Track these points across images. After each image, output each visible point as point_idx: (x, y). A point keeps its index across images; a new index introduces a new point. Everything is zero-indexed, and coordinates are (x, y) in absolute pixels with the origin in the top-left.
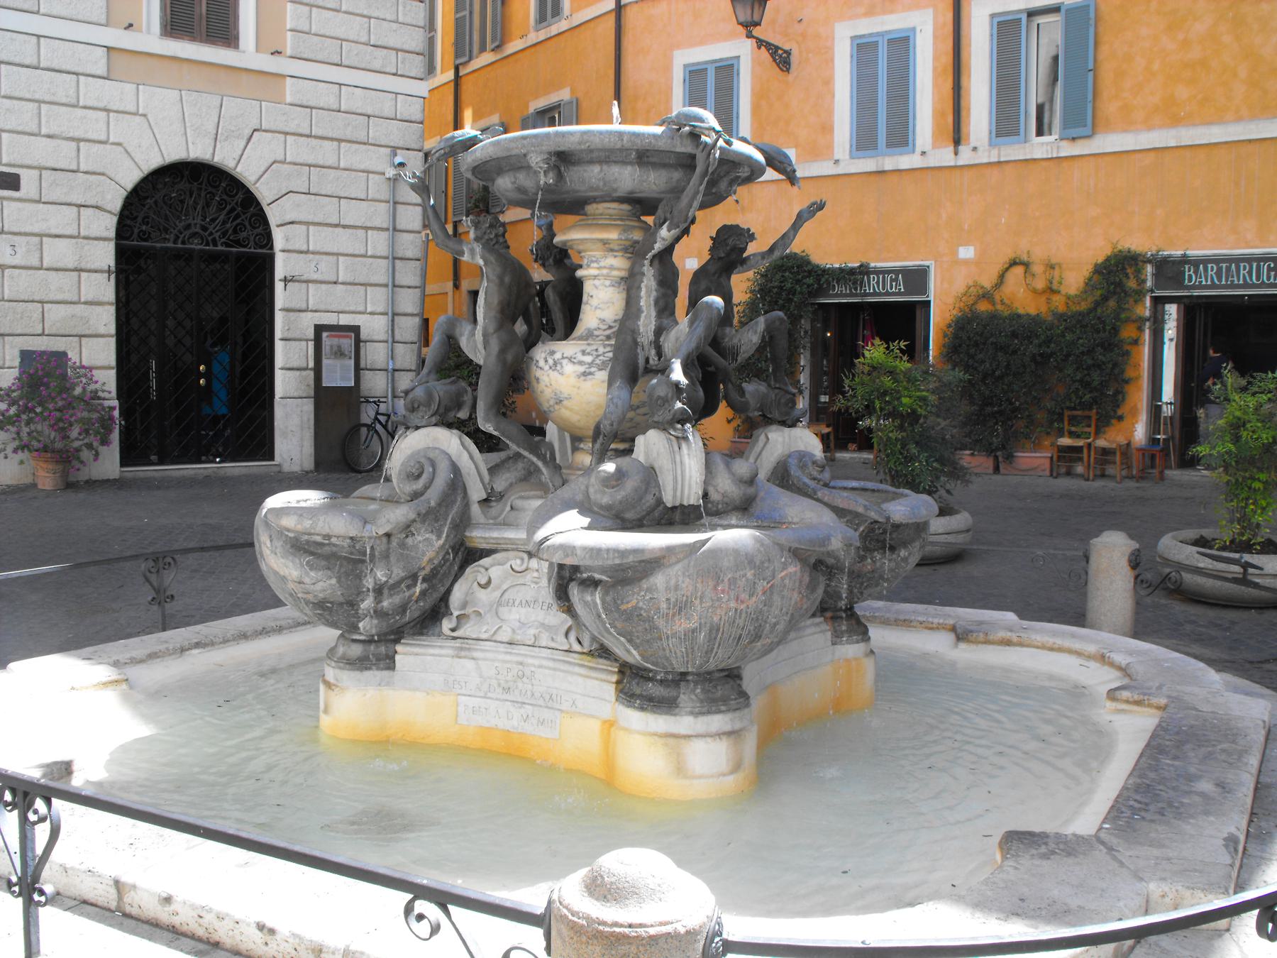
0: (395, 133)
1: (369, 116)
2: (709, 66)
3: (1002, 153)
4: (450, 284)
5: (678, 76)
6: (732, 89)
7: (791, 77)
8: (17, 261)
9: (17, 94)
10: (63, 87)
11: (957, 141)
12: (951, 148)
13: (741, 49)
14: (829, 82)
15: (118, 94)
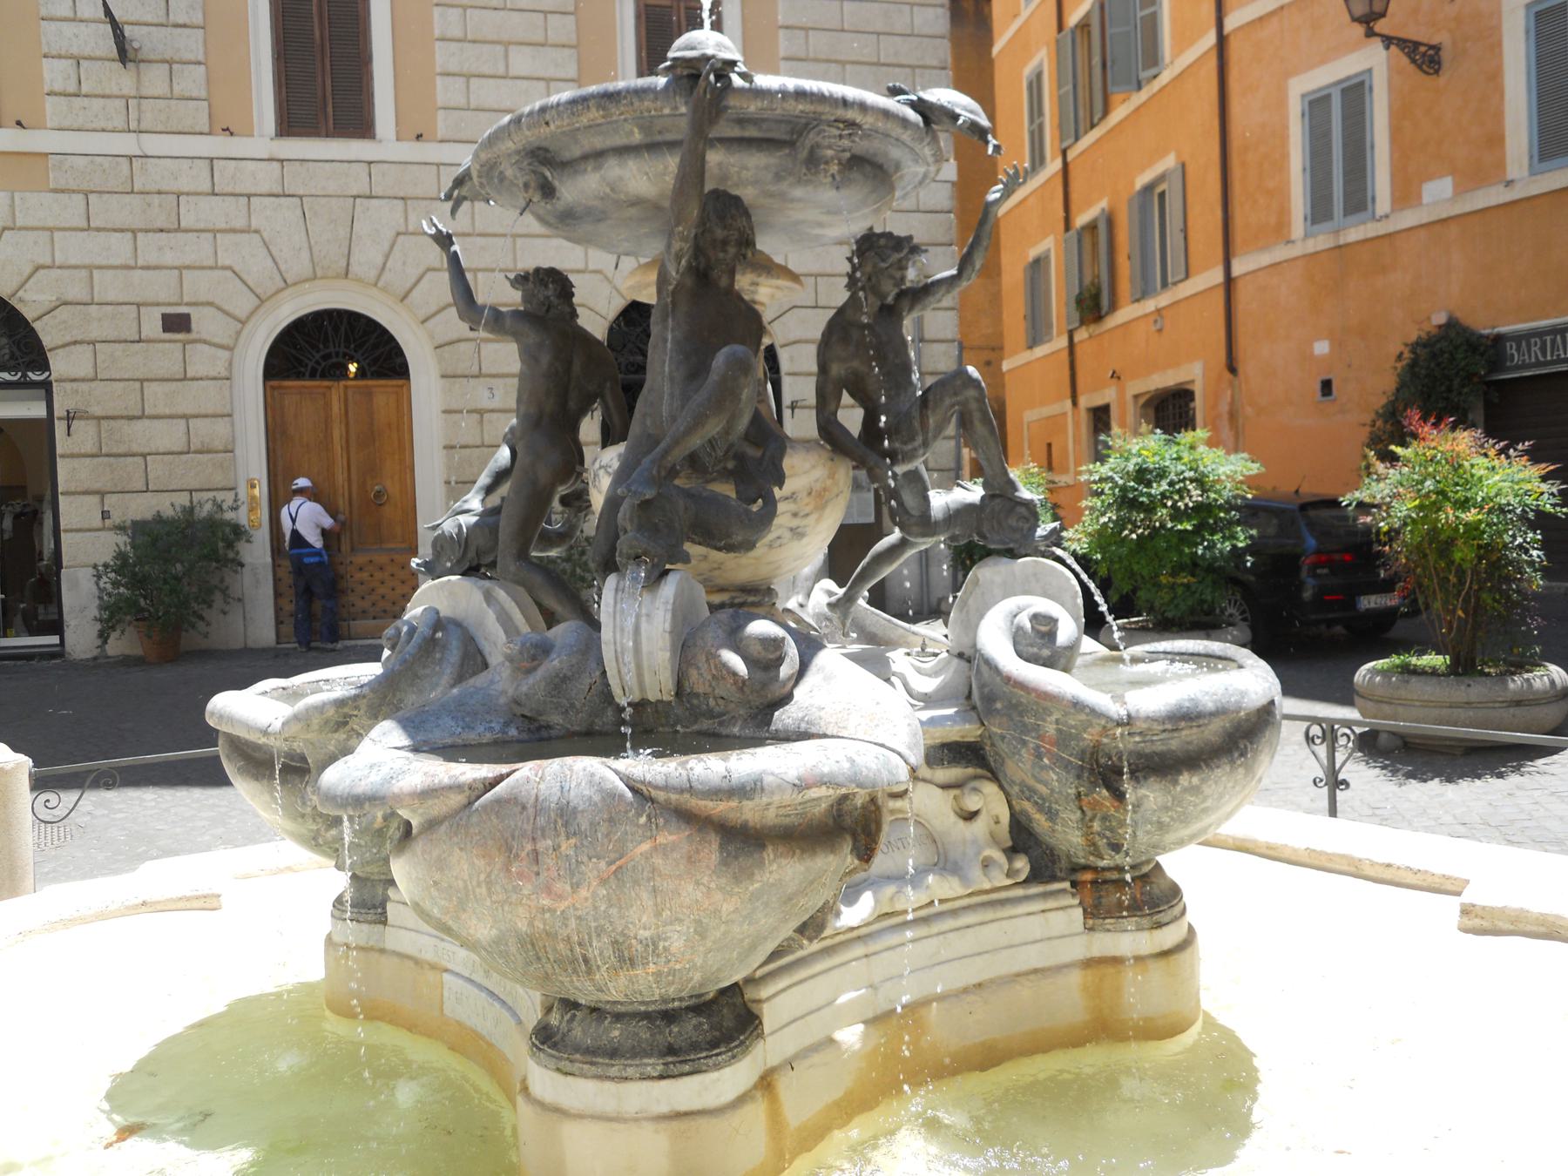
2: (1332, 90)
4: (1069, 403)
5: (1295, 108)
6: (1363, 113)
7: (1442, 79)
8: (496, 404)
9: (490, 230)
13: (1373, 60)
14: (1495, 77)
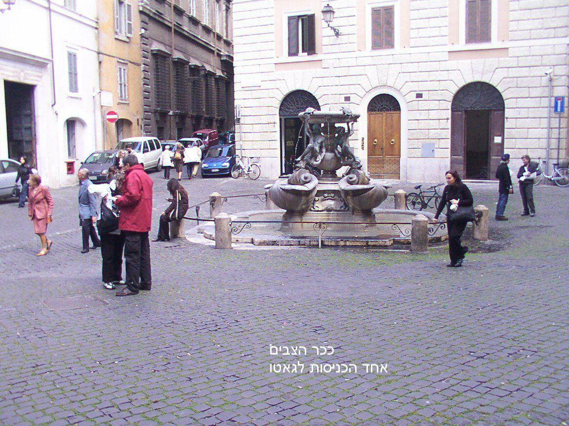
0: (553, 60)
1: (542, 56)
10: (435, 66)
15: (452, 64)
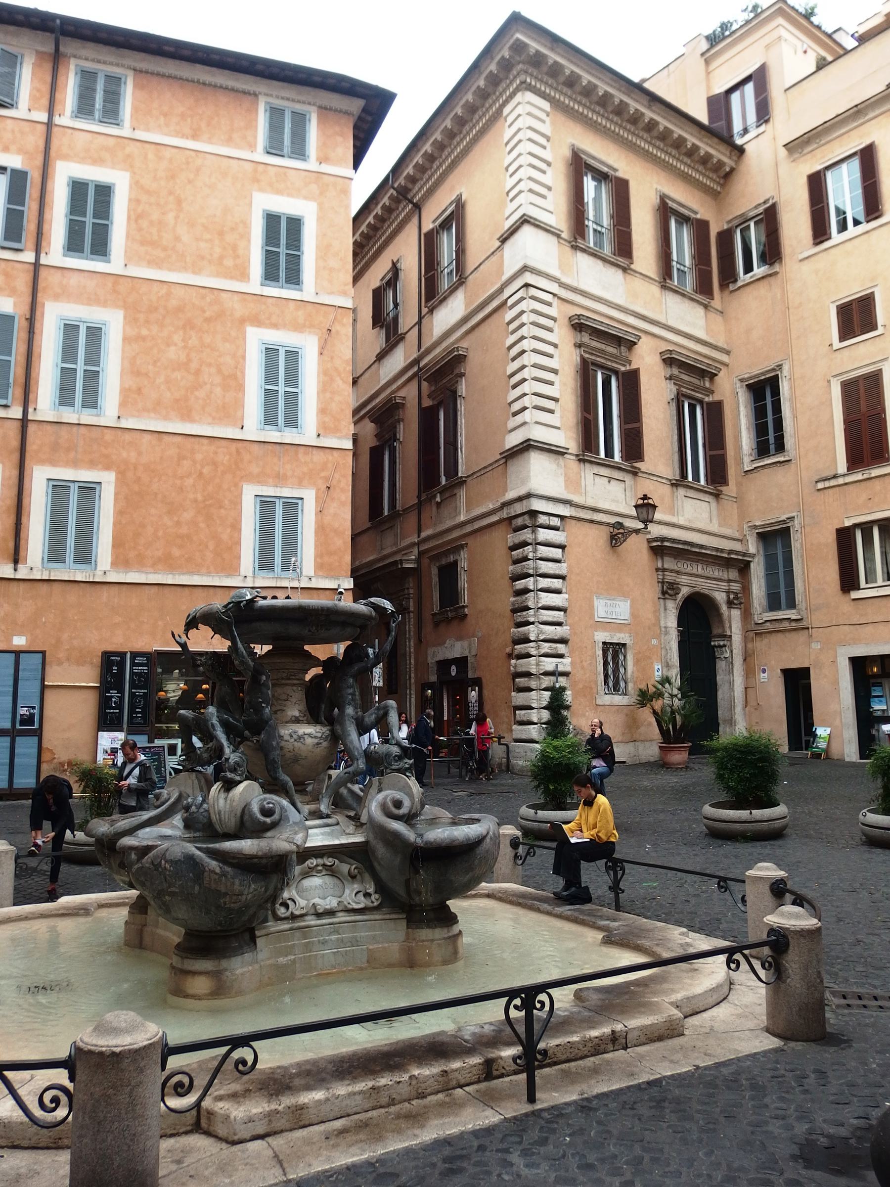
3: (52, 574)
11: (16, 561)
12: (12, 565)
